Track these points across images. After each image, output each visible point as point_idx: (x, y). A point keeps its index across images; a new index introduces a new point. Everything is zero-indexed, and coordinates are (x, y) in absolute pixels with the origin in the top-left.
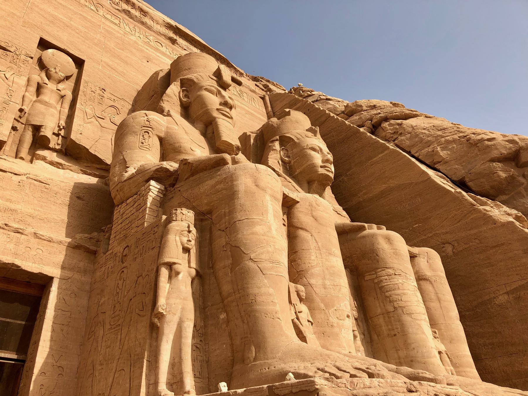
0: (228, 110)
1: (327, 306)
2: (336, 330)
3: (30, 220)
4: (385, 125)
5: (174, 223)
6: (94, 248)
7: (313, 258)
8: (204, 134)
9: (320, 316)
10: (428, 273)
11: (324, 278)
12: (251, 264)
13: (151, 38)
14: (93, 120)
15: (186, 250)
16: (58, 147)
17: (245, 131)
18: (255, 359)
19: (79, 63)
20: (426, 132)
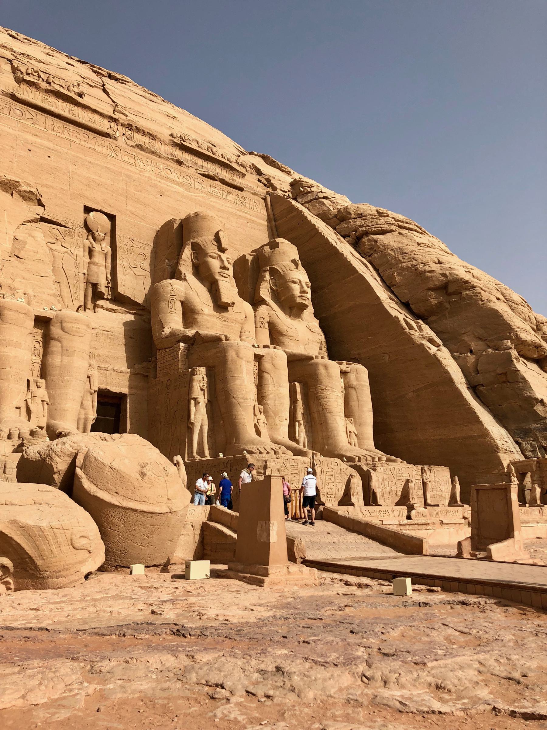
0: (226, 272)
1: (276, 415)
2: (278, 427)
3: (108, 359)
4: (365, 239)
5: (195, 376)
6: (147, 374)
7: (270, 389)
8: (210, 291)
9: (271, 420)
10: (354, 383)
11: (275, 400)
12: (234, 400)
13: (161, 166)
14: (129, 271)
15: (202, 390)
16: (109, 297)
17: (245, 253)
18: (235, 443)
19: (112, 218)
20: (393, 254)
